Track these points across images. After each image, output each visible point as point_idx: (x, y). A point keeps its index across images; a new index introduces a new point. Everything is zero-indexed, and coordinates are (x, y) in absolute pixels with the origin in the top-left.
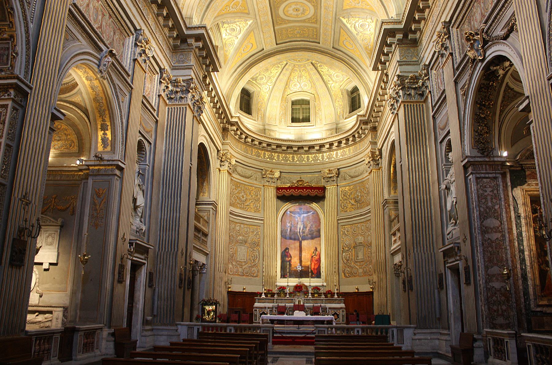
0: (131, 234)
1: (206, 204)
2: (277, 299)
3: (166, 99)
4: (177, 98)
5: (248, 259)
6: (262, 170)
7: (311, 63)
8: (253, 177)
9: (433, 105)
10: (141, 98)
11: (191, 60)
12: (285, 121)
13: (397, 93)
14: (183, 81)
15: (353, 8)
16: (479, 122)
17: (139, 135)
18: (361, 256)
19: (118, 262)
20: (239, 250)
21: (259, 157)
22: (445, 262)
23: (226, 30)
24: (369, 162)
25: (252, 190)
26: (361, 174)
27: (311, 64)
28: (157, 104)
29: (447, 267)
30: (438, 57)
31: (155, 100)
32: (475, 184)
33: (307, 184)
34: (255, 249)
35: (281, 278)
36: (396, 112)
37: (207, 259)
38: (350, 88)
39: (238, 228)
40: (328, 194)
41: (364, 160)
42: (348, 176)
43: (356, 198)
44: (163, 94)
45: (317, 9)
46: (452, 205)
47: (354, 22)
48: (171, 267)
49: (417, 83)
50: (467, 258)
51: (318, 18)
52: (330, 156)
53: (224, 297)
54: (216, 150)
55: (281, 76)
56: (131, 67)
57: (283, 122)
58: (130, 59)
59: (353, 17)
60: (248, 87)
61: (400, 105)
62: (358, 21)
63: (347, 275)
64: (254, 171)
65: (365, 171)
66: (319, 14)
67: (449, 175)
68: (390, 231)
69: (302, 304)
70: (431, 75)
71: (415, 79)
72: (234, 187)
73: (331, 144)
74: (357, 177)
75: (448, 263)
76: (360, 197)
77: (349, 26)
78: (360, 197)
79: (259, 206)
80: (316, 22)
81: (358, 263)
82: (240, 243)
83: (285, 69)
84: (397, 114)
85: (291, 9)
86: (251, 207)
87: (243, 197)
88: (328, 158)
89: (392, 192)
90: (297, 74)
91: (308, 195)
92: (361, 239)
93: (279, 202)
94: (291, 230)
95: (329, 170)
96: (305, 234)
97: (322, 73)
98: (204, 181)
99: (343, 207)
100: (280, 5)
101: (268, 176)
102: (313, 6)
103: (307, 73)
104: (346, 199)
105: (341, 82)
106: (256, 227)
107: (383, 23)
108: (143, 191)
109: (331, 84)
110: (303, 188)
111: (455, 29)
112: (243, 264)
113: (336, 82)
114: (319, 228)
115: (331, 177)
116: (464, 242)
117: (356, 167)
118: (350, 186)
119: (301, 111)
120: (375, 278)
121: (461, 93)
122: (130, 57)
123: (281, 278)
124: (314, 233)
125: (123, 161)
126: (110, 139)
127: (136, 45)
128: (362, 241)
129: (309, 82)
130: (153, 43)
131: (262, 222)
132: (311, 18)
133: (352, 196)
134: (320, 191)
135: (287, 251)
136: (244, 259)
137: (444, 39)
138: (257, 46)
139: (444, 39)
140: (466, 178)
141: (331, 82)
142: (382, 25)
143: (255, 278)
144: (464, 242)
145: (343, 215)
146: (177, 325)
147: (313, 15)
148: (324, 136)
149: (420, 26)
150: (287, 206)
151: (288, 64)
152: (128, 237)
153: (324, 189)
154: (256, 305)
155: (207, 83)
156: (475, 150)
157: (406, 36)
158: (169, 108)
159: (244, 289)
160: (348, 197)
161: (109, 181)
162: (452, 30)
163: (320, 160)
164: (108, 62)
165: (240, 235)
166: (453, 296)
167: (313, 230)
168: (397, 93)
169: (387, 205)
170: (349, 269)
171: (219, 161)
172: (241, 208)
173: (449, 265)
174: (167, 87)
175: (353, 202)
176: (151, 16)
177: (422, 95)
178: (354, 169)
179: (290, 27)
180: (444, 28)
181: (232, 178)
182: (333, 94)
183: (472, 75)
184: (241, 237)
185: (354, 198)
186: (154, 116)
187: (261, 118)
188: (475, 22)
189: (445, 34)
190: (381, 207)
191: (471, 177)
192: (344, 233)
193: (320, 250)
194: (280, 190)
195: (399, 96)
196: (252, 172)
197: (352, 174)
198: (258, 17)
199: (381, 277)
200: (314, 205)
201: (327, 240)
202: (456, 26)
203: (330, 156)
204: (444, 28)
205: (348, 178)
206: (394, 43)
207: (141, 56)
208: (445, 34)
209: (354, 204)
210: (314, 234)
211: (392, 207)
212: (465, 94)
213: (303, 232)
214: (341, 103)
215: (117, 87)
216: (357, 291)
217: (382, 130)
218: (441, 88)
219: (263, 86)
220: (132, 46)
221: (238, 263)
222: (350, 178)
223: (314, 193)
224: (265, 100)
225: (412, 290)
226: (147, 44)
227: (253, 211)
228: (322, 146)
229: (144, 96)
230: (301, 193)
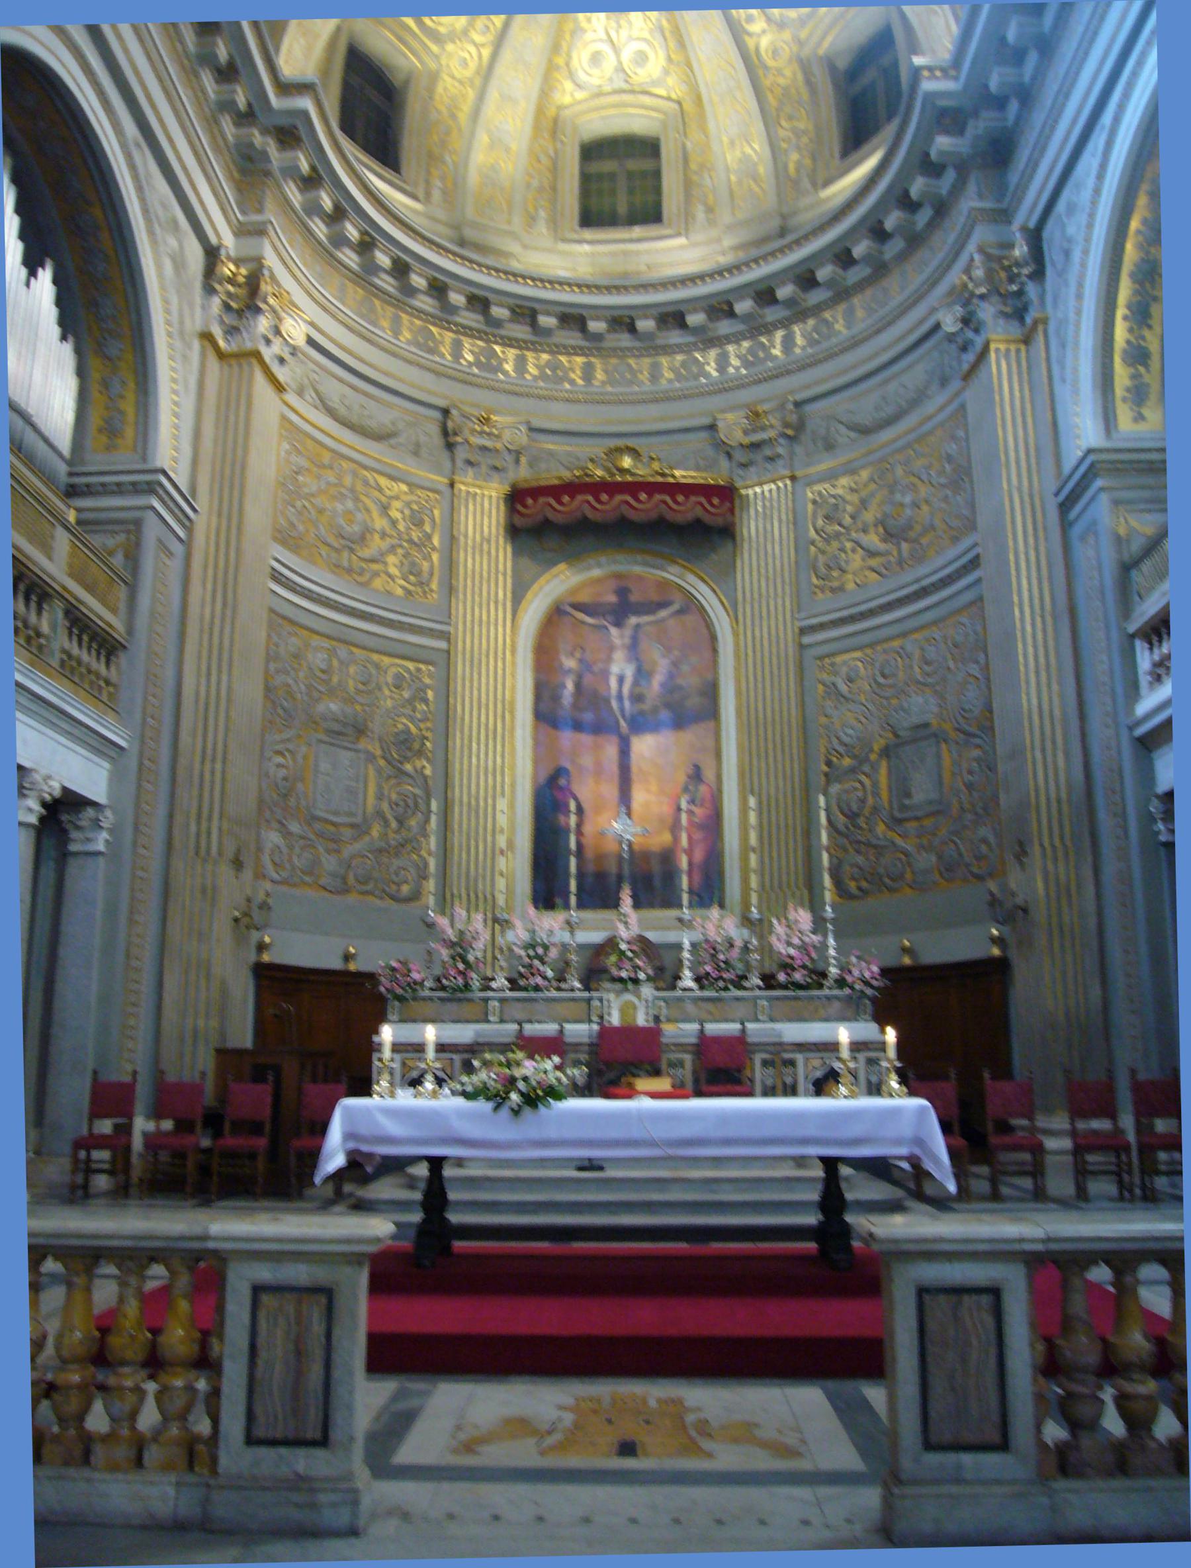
2: (502, 1000)
5: (370, 809)
8: (401, 440)
12: (554, 223)
18: (922, 791)
20: (324, 766)
21: (431, 351)
25: (397, 498)
34: (408, 767)
37: (115, 778)
39: (318, 659)
40: (750, 526)
41: (937, 327)
52: (755, 355)
68: (1126, 610)
69: (641, 1020)
73: (765, 295)
78: (908, 512)
81: (911, 826)
82: (329, 732)
86: (393, 571)
87: (351, 522)
88: (746, 364)
93: (525, 561)
95: (757, 414)
96: (646, 706)
104: (838, 535)
106: (411, 665)
110: (634, 488)
112: (347, 833)
114: (709, 677)
117: (886, 382)
118: (853, 472)
119: (622, 184)
131: (443, 645)
133: (869, 516)
134: (716, 501)
135: (562, 782)
145: (825, 606)
153: (727, 494)
159: (347, 957)
160: (847, 520)
163: (707, 375)
167: (680, 688)
172: (336, 568)
175: (873, 539)
185: (881, 522)
187: (445, 192)
192: (832, 691)
194: (530, 501)
199: (1062, 877)
201: (747, 725)
203: (755, 355)
213: (637, 698)
214: (802, 125)
216: (907, 961)
217: (1041, 147)
219: (450, 47)
222: (853, 434)
223: (687, 510)
224: (463, 117)
227: (400, 592)
230: (625, 510)
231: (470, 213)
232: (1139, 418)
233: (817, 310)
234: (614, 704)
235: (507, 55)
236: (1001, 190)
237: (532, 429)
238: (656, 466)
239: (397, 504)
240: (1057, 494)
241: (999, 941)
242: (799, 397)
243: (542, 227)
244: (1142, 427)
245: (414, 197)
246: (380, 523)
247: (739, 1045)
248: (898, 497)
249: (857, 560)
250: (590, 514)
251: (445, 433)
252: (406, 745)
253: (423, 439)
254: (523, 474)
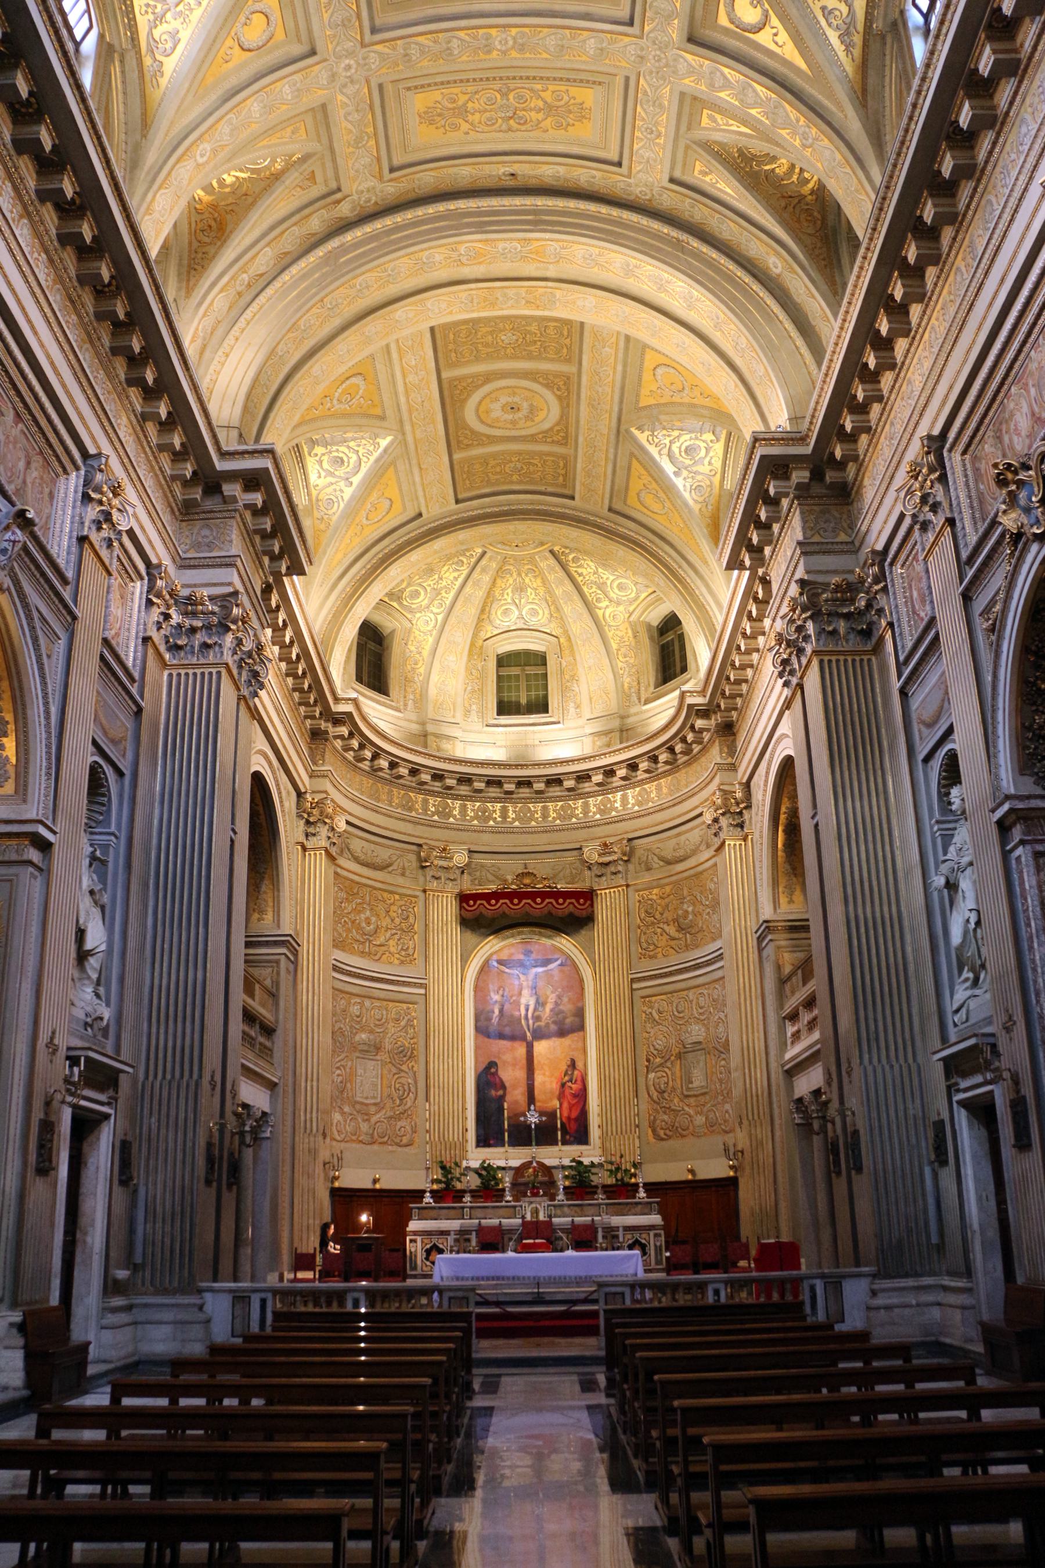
0: (71, 1033)
1: (267, 944)
2: (471, 1208)
3: (162, 648)
4: (193, 647)
5: (385, 1094)
6: (420, 845)
7: (552, 552)
8: (394, 867)
9: (902, 658)
10: (98, 647)
11: (231, 541)
12: (482, 714)
13: (800, 629)
14: (212, 598)
15: (665, 405)
16: (1034, 703)
17: (91, 748)
18: (698, 1080)
19: (38, 1115)
20: (360, 1071)
21: (410, 809)
22: (949, 1088)
23: (320, 462)
24: (716, 820)
25: (393, 904)
26: (694, 852)
27: (549, 555)
28: (138, 662)
29: (959, 1102)
30: (910, 530)
31: (135, 652)
32: (1032, 869)
33: (546, 883)
34: (404, 1067)
35: (478, 1146)
36: (794, 681)
38: (656, 616)
39: (355, 1010)
41: (701, 814)
42: (656, 859)
43: (681, 920)
44: (157, 637)
45: (568, 405)
46: (966, 933)
47: (667, 441)
48: (181, 1123)
49: (852, 601)
50: (1017, 1074)
51: (572, 430)
53: (321, 1209)
54: (294, 794)
55: (468, 589)
56: (73, 558)
57: (474, 713)
58: (70, 538)
59: (664, 428)
60: (378, 619)
61: (809, 662)
62: (678, 437)
63: (662, 1133)
64: (397, 849)
65: (703, 847)
66: (572, 420)
67: (952, 849)
69: (541, 1217)
70: (892, 580)
71: (849, 590)
72: (343, 895)
73: (609, 772)
74: (681, 861)
75: (958, 1091)
76: (690, 917)
77: (653, 451)
79: (411, 946)
80: (564, 442)
81: (692, 1100)
83: (478, 569)
84: (800, 686)
85: (497, 406)
86: (392, 949)
87: (369, 924)
88: (602, 812)
89: (783, 900)
90: (511, 581)
91: (550, 913)
92: (696, 1032)
93: (471, 937)
94: (501, 1011)
95: (605, 845)
96: (542, 1024)
97: (579, 579)
98: (262, 879)
99: (645, 945)
100: (469, 396)
101: (436, 862)
102: (560, 398)
103: (539, 581)
105: (631, 602)
106: (405, 1006)
107: (756, 440)
108: (103, 908)
109: (606, 610)
110: (533, 895)
111: (957, 456)
112: (373, 1109)
113: (618, 604)
115: (607, 864)
116: (1008, 1030)
117: (679, 835)
118: (662, 887)
119: (523, 685)
120: (741, 1138)
121: (981, 625)
122: (71, 531)
123: (478, 1146)
124: (565, 1018)
125: (49, 823)
126: (13, 760)
127: (86, 498)
128: (701, 1039)
129: (544, 605)
130: (130, 493)
131: (422, 991)
132: (551, 429)
133: (669, 915)
136: (374, 1097)
137: (928, 483)
138: (404, 504)
139: (928, 483)
140: (1006, 855)
141: (603, 604)
142: (754, 447)
143: (407, 1149)
144: (1008, 1030)
145: (647, 966)
146: (200, 1291)
147: (558, 424)
148: (588, 751)
149: (856, 450)
150: (492, 946)
151: (487, 556)
152: (63, 1041)
153: (588, 896)
154: (413, 1225)
155: (274, 604)
156: (1026, 778)
157: (817, 475)
158: (170, 675)
160: (658, 916)
161: (11, 881)
162: (950, 459)
163: (576, 816)
164: (14, 542)
165: (362, 1029)
166: (977, 1180)
167: (561, 1012)
168: (800, 629)
169: (770, 937)
170: (666, 1117)
171: (302, 822)
172: (362, 954)
173: (962, 1096)
174: (167, 617)
175: (672, 930)
176: (124, 419)
177: (866, 634)
178: (674, 841)
179: (494, 456)
180: (928, 453)
181: (339, 870)
182: (610, 634)
183: (1013, 575)
184: (363, 1036)
185: (674, 920)
186: (131, 697)
187: (415, 702)
188: (1015, 438)
189: (932, 470)
190: (753, 942)
191: (1020, 851)
193: (585, 1065)
195: (807, 638)
196: (391, 851)
197: (668, 854)
198: (408, 428)
200: (565, 943)
201: (600, 1038)
202: (961, 447)
204: (928, 453)
205: (656, 863)
206: (787, 495)
207: (99, 529)
208: (932, 470)
209: (676, 935)
210: (568, 1021)
211: (783, 943)
212: (996, 629)
213: (537, 1019)
215: (35, 615)
216: (690, 1177)
218: (922, 614)
219: (418, 615)
220: (75, 501)
221: (358, 1107)
223: (566, 907)
225: (859, 1169)
226: (116, 495)
227: (396, 962)
228: (583, 777)
229: (106, 642)
231: (431, 715)
232: (791, 902)
233: (642, 782)
234: (523, 1022)
235: (452, 620)
236: (732, 751)
237: (470, 851)
238: (546, 883)
239: (393, 908)
241: (731, 1167)
242: (631, 836)
243: (474, 716)
244: (793, 906)
245: (398, 710)
246: (386, 922)
247: (592, 1228)
248: (685, 906)
249: (663, 941)
250: (507, 910)
251: (420, 860)
252: (404, 1055)
253: (407, 865)
254: (467, 885)
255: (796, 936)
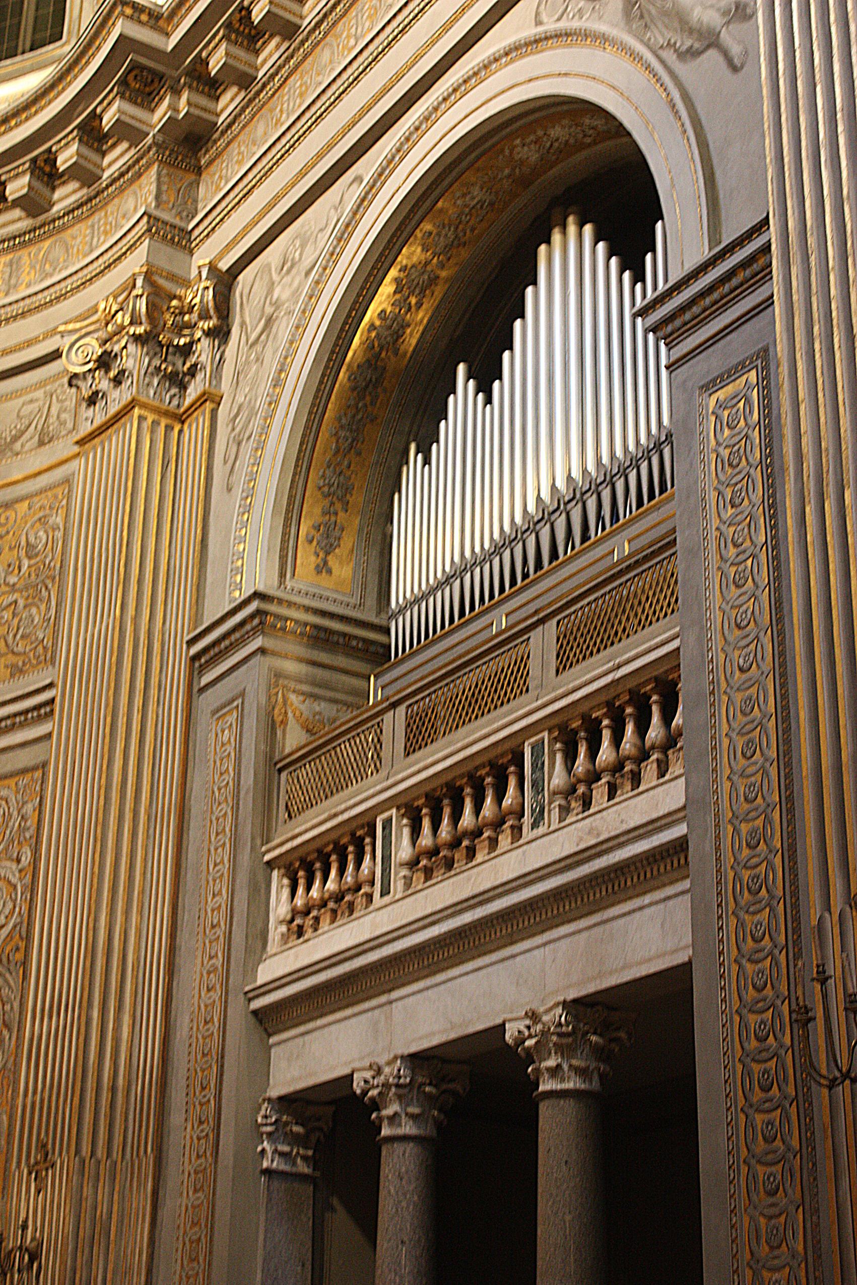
24: (104, 362)
41: (56, 355)
89: (307, 558)
190: (178, 669)
211: (291, 667)
232: (323, 568)
240: (191, 642)
244: (324, 580)
255: (323, 657)
